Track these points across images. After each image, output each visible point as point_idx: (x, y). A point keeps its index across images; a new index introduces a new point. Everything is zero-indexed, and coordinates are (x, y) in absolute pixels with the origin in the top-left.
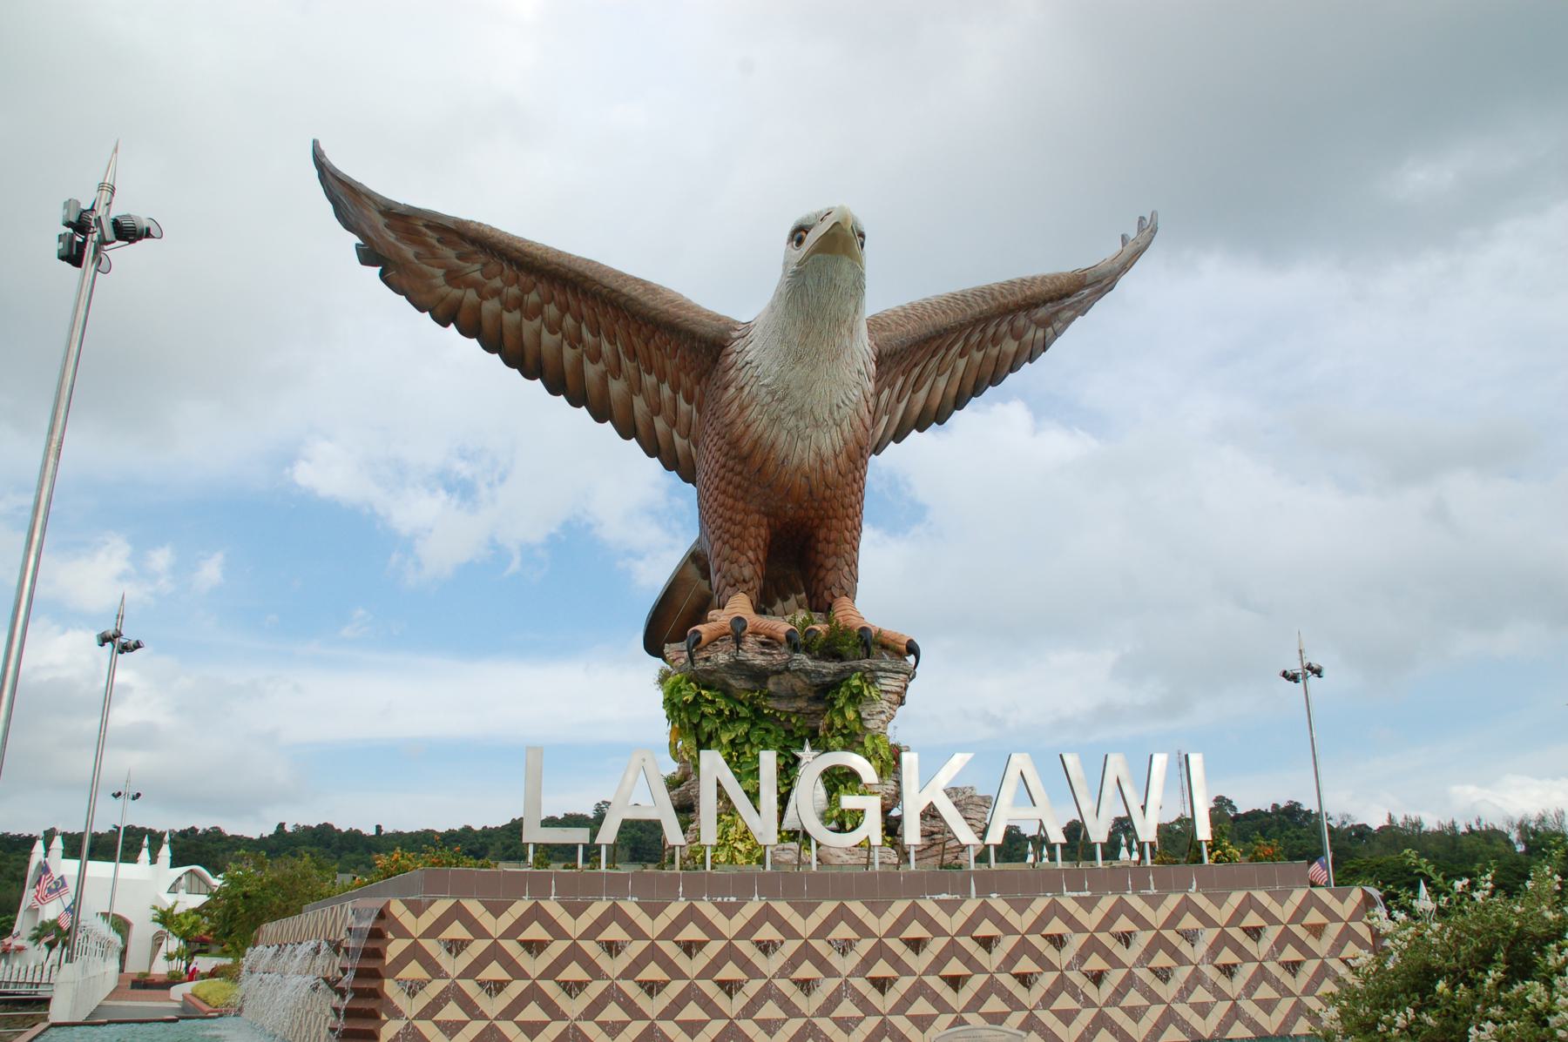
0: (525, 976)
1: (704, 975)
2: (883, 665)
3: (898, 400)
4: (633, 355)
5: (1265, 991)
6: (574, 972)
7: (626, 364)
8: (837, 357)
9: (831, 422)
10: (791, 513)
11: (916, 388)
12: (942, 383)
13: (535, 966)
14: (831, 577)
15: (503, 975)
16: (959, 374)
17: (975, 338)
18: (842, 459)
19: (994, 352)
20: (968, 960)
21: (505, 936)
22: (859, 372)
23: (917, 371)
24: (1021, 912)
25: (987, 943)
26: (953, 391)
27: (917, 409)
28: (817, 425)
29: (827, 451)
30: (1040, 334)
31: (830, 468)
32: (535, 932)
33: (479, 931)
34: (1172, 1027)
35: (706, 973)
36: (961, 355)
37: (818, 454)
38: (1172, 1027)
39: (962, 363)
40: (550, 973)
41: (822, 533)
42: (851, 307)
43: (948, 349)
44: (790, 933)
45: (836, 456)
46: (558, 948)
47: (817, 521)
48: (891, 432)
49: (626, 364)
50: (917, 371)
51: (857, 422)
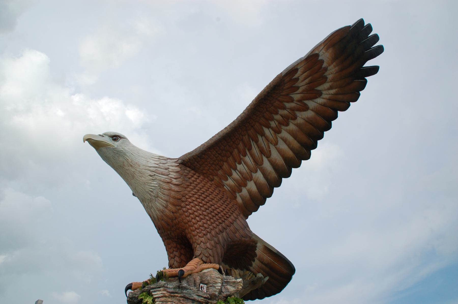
2: (152, 286)
3: (258, 164)
8: (133, 177)
9: (153, 198)
10: (173, 234)
11: (266, 153)
12: (283, 146)
16: (290, 138)
17: (273, 124)
18: (170, 206)
19: (299, 121)
22: (150, 176)
23: (255, 150)
26: (296, 144)
27: (280, 160)
28: (151, 201)
29: (161, 208)
30: (320, 100)
31: (167, 212)
36: (277, 131)
37: (158, 211)
39: (284, 134)
41: (189, 236)
42: (121, 159)
43: (263, 134)
45: (166, 207)
47: (183, 233)
48: (273, 174)
50: (255, 150)
51: (166, 192)
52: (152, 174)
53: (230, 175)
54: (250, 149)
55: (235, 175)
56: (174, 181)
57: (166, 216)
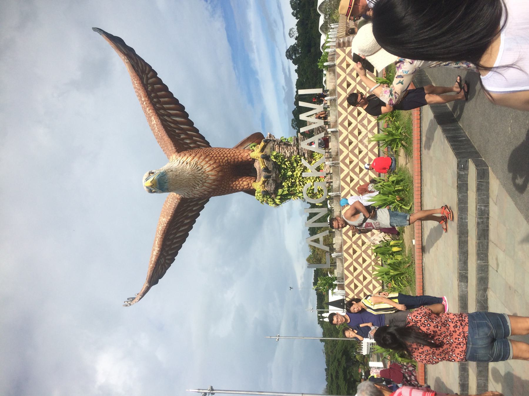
0: (358, 162)
1: (356, 120)
4: (183, 214)
5: (366, 141)
6: (361, 278)
7: (185, 214)
13: (359, 269)
14: (244, 159)
15: (358, 167)
18: (211, 162)
20: (354, 129)
21: (353, 276)
24: (342, 133)
25: (350, 124)
32: (351, 269)
33: (352, 281)
34: (374, 150)
35: (362, 283)
38: (374, 150)
40: (361, 266)
44: (348, 174)
46: (356, 281)
49: (185, 214)
50: (172, 125)
51: (201, 160)
52: (185, 163)
53: (187, 144)
54: (171, 127)
55: (188, 141)
56: (193, 155)
57: (217, 167)
